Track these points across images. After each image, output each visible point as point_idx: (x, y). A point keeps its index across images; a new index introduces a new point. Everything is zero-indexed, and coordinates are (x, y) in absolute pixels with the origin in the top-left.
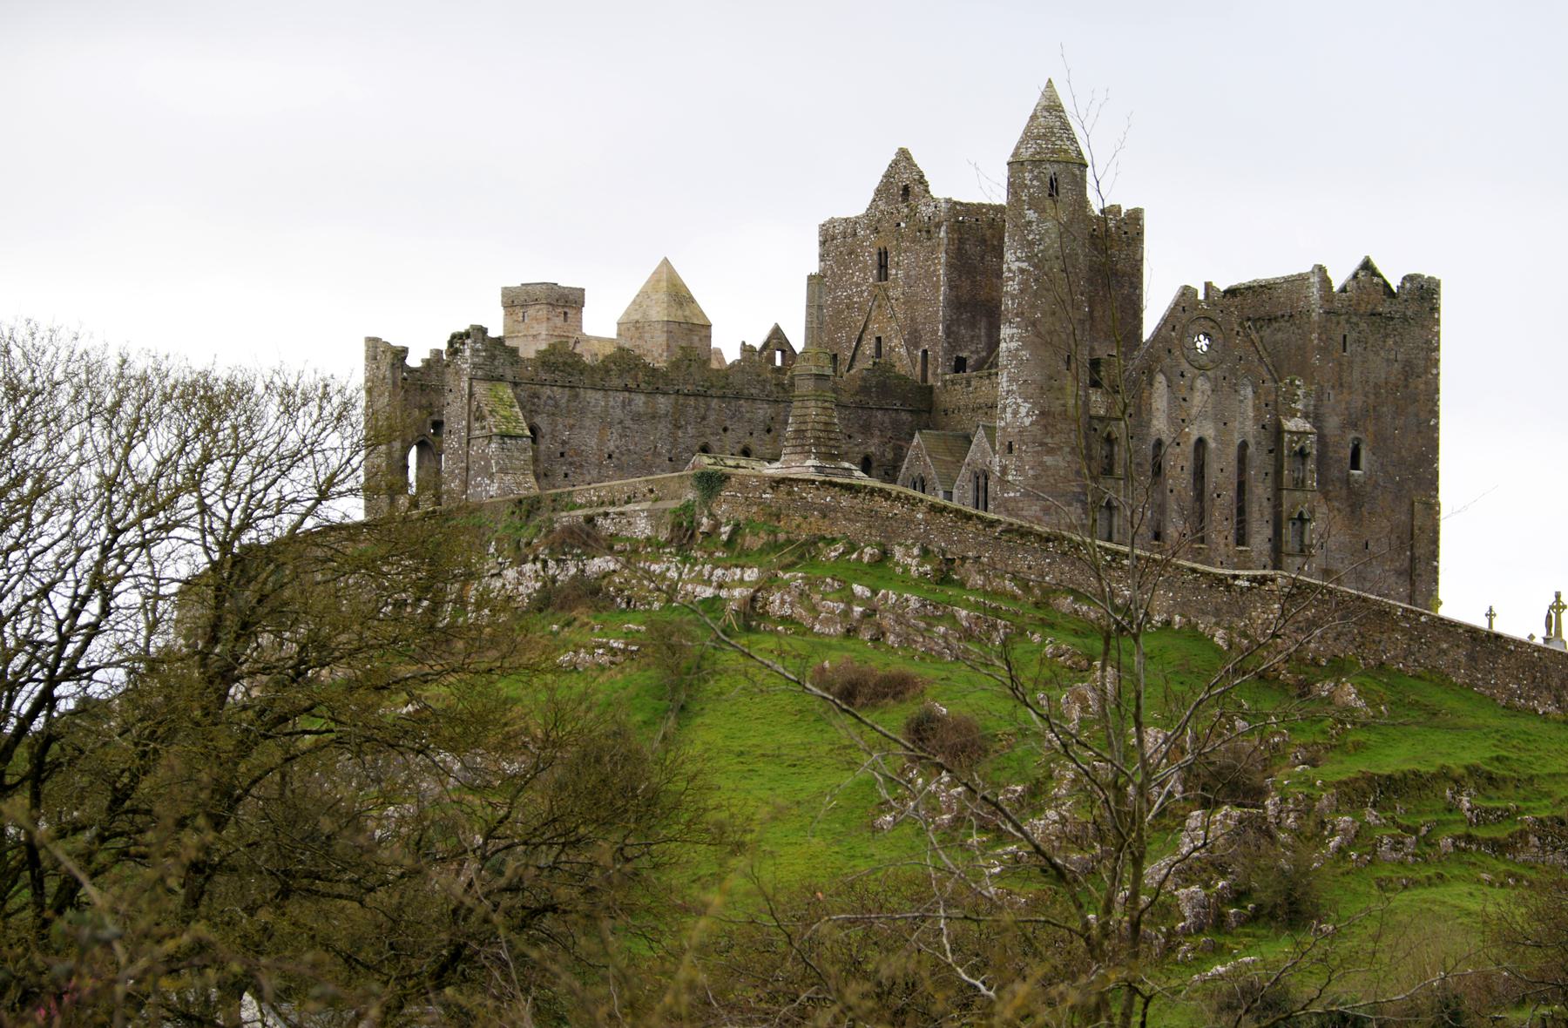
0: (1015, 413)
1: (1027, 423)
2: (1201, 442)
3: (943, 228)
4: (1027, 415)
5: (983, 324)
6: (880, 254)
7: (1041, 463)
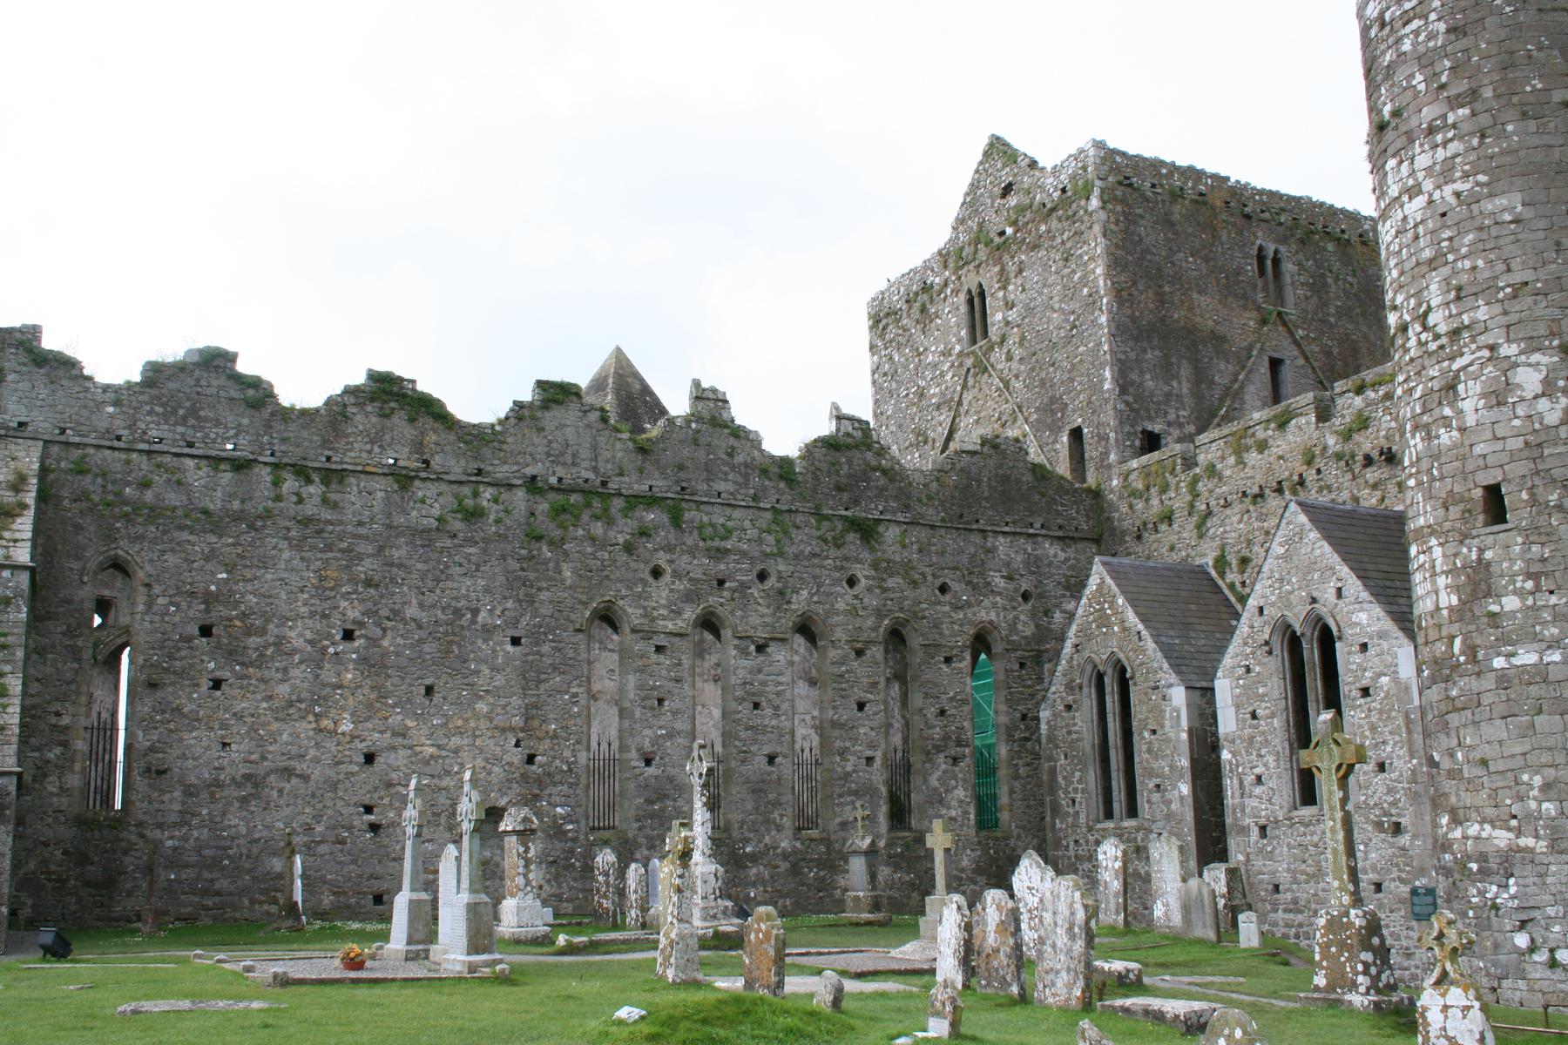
0: (1497, 397)
1: (1553, 418)
5: (1185, 371)
6: (970, 302)
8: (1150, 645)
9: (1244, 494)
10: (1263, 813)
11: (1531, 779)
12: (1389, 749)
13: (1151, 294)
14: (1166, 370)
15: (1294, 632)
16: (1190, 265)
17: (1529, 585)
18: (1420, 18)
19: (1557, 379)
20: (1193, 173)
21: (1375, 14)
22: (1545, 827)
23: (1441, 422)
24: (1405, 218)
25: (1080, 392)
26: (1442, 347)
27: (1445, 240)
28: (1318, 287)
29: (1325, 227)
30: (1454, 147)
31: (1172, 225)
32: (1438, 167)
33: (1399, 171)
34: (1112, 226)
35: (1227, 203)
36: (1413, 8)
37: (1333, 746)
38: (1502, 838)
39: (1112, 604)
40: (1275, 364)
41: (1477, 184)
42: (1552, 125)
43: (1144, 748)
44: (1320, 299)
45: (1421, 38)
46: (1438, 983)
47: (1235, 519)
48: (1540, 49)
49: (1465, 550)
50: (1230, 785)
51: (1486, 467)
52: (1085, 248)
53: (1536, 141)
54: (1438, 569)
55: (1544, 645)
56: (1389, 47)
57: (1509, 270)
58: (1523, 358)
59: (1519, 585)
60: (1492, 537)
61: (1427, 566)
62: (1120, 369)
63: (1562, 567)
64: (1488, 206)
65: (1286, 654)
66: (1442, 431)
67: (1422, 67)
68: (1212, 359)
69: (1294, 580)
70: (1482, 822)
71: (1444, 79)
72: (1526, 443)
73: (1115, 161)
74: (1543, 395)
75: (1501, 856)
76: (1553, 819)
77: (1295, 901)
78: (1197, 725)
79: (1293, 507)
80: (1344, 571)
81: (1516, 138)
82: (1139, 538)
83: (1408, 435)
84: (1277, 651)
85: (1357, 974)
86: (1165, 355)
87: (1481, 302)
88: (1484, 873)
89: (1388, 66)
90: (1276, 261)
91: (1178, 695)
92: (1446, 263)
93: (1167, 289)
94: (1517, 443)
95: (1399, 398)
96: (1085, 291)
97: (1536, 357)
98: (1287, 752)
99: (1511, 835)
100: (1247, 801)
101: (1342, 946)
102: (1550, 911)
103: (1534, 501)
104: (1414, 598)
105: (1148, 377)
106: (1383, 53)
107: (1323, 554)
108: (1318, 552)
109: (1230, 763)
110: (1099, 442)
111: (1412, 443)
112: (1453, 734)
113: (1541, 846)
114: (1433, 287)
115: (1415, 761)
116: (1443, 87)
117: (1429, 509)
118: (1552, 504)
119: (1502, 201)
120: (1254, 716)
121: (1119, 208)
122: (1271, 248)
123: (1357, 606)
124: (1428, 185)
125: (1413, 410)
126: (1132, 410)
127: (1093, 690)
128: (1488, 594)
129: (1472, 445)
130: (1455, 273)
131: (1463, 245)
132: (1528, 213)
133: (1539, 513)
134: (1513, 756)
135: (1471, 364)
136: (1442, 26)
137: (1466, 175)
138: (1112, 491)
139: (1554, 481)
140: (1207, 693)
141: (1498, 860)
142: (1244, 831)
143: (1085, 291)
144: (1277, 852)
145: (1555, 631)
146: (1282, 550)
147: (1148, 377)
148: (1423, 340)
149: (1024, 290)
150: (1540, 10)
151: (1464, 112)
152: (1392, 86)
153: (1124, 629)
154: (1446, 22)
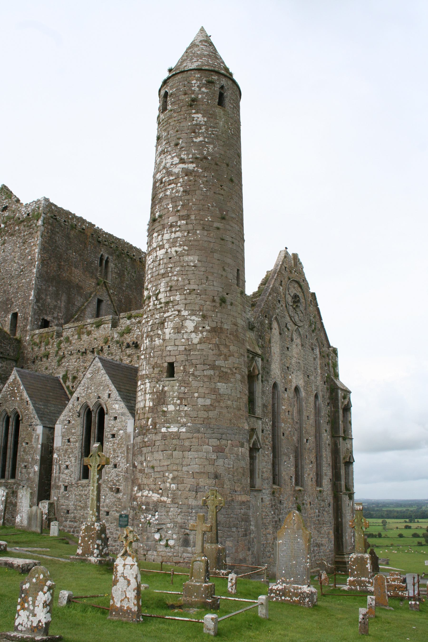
0: (178, 329)
1: (196, 341)
2: (297, 389)
3: (42, 218)
4: (196, 330)
5: (64, 298)
7: (214, 391)
8: (31, 407)
9: (79, 351)
10: (67, 481)
11: (169, 475)
12: (119, 459)
13: (56, 264)
14: (56, 296)
15: (90, 409)
16: (73, 255)
17: (178, 402)
18: (174, 184)
19: (199, 327)
20: (81, 220)
21: (160, 178)
22: (171, 494)
23: (157, 336)
24: (157, 256)
25: (20, 298)
26: (161, 307)
27: (169, 267)
28: (121, 275)
29: (127, 252)
30: (178, 234)
31: (69, 238)
32: (171, 240)
33: (157, 238)
34: (45, 234)
35: (92, 235)
36: (173, 180)
37: (97, 457)
38: (155, 497)
39: (18, 388)
40: (100, 302)
41: (184, 249)
42: (212, 234)
43: (22, 450)
44: (121, 280)
45: (174, 191)
46: (123, 555)
47: (74, 360)
48: (212, 206)
49: (158, 386)
50: (55, 468)
51: (170, 355)
52: (33, 240)
53: (206, 239)
54: (147, 392)
55: (180, 425)
56: (162, 192)
57: (189, 284)
58: (189, 317)
59: (175, 401)
60: (168, 382)
61: (143, 390)
62: (38, 292)
63: (191, 397)
64: (186, 258)
65: (85, 417)
66: (157, 339)
67: (172, 202)
68: (75, 295)
69: (93, 388)
70: (149, 491)
71: (179, 208)
72: (185, 349)
73: (51, 208)
74: (194, 332)
75: (154, 504)
76: (174, 491)
77: (75, 517)
78: (45, 442)
79: (97, 359)
80: (113, 387)
81: (199, 236)
82: (34, 362)
83: (144, 338)
84: (82, 416)
85: (94, 549)
86: (57, 289)
87: (178, 293)
88: (147, 510)
89: (161, 198)
90: (107, 262)
91: (40, 429)
92: (168, 276)
93: (62, 263)
94: (182, 348)
95: (143, 324)
96: (30, 257)
97: (193, 317)
98: (80, 456)
99: (159, 496)
100: (61, 475)
101: (90, 537)
102: (169, 525)
103: (185, 371)
104: (137, 402)
105: (49, 297)
106: (160, 193)
107: (105, 380)
108: (104, 379)
109: (57, 459)
110: (24, 320)
111: (145, 342)
112: (143, 456)
113: (169, 501)
114: (162, 284)
115: (128, 465)
116: (178, 211)
117: (147, 368)
118: (191, 373)
119: (191, 258)
120: (69, 441)
121: (49, 227)
122: (106, 256)
123: (115, 402)
124: (167, 246)
125: (148, 329)
126: (40, 309)
127: (4, 423)
128: (163, 404)
129: (166, 346)
130: (171, 281)
131: (175, 271)
132: (199, 264)
133: (186, 375)
134: (163, 466)
135: (170, 316)
136: (181, 189)
137: (180, 246)
138: (26, 341)
139: (193, 364)
140: (52, 429)
141: (153, 505)
142: (58, 487)
143: (30, 257)
144: (70, 497)
145: (185, 420)
146: (90, 376)
147: (49, 297)
148: (155, 303)
149: (4, 251)
150: (215, 193)
151: (184, 222)
152: (160, 206)
153: (21, 399)
154: (183, 188)
